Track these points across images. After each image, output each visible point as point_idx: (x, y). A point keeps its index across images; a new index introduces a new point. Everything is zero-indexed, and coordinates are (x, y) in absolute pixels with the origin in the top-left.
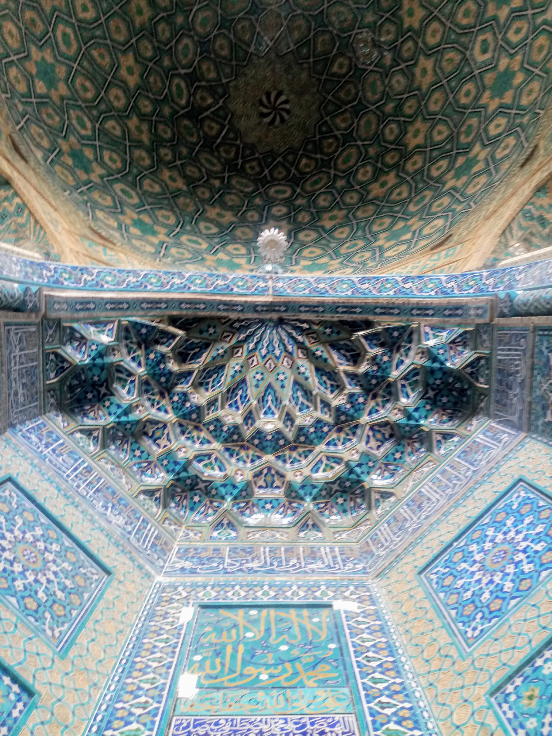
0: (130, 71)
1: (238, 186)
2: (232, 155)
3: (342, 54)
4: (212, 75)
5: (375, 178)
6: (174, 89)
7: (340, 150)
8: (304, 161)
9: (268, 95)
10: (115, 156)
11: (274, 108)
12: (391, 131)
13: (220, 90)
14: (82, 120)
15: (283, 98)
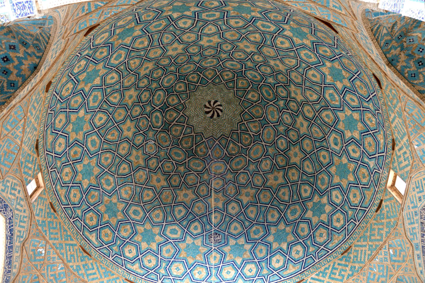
0: (129, 129)
1: (194, 167)
2: (190, 144)
3: (254, 91)
4: (176, 101)
5: (271, 171)
6: (154, 120)
7: (252, 144)
8: (231, 145)
9: (209, 102)
10: (127, 188)
11: (213, 108)
12: (282, 144)
13: (180, 107)
14: (108, 180)
15: (218, 103)
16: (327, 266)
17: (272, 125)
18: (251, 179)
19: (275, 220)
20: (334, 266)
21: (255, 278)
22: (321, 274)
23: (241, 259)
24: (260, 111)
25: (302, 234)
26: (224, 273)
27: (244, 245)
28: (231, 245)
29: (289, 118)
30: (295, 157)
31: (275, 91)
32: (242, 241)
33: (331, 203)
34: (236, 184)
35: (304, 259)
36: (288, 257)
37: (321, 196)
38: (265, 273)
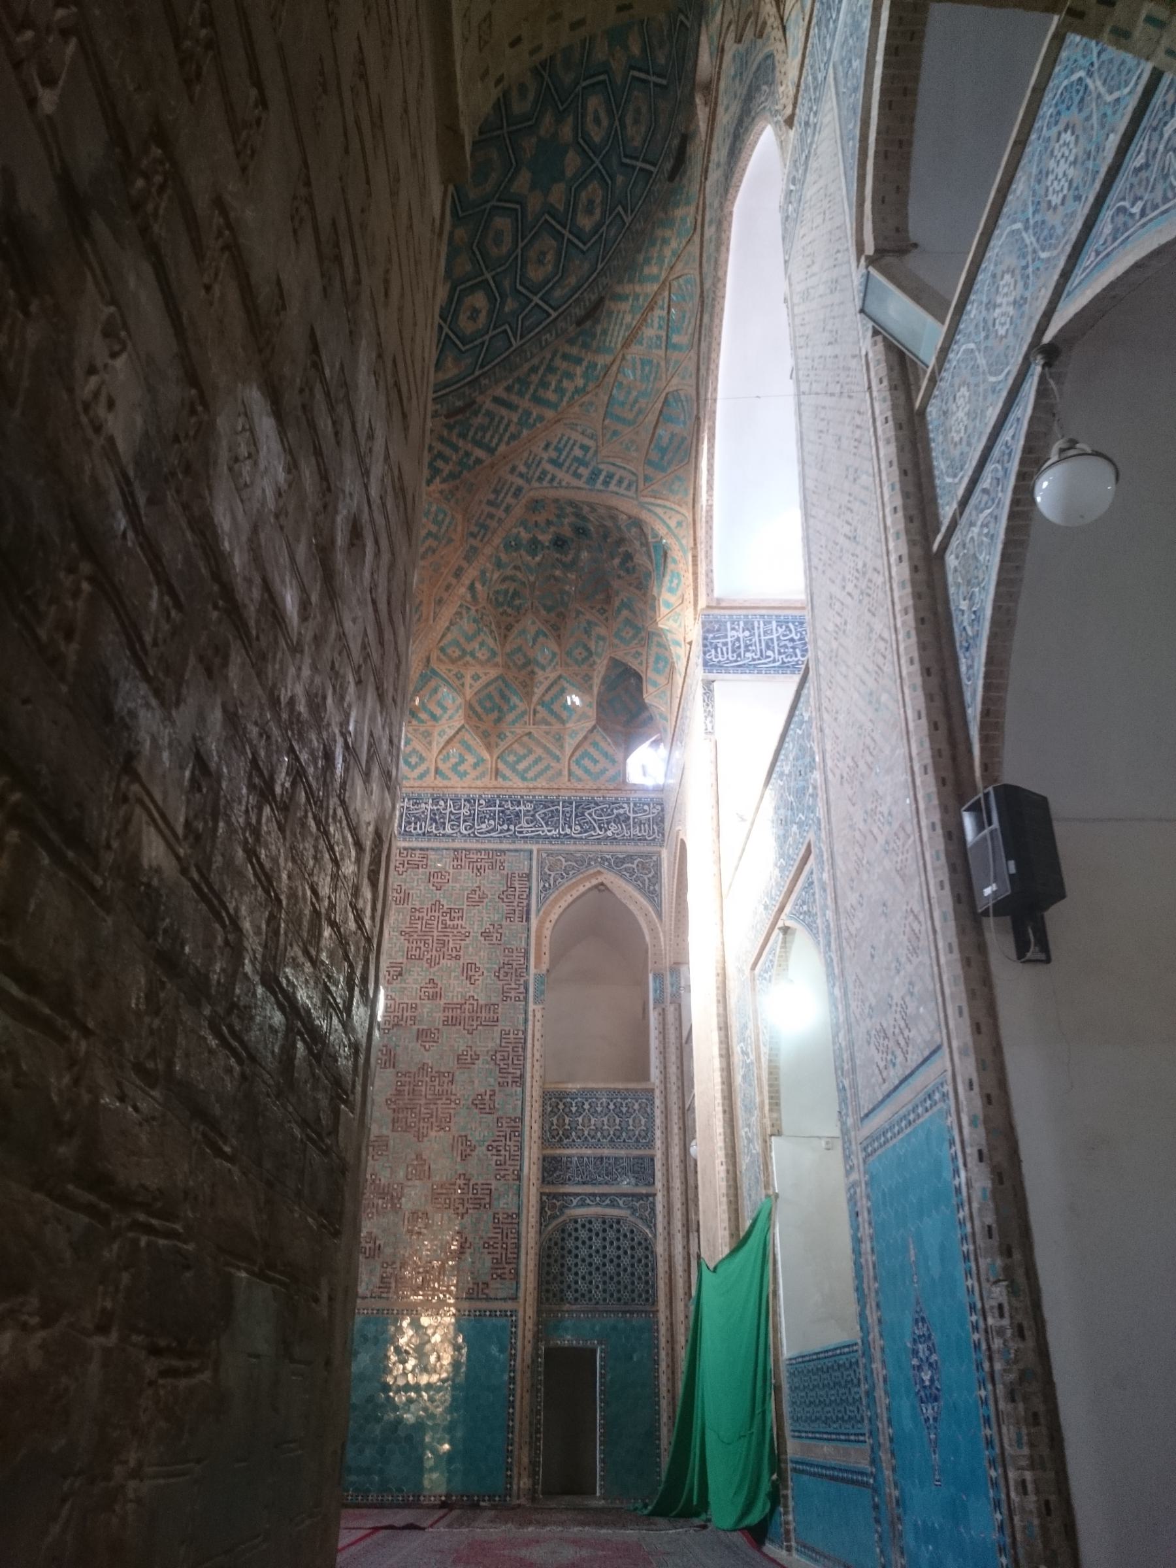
16: (535, 361)
20: (552, 360)
22: (517, 386)
25: (494, 252)
35: (487, 338)
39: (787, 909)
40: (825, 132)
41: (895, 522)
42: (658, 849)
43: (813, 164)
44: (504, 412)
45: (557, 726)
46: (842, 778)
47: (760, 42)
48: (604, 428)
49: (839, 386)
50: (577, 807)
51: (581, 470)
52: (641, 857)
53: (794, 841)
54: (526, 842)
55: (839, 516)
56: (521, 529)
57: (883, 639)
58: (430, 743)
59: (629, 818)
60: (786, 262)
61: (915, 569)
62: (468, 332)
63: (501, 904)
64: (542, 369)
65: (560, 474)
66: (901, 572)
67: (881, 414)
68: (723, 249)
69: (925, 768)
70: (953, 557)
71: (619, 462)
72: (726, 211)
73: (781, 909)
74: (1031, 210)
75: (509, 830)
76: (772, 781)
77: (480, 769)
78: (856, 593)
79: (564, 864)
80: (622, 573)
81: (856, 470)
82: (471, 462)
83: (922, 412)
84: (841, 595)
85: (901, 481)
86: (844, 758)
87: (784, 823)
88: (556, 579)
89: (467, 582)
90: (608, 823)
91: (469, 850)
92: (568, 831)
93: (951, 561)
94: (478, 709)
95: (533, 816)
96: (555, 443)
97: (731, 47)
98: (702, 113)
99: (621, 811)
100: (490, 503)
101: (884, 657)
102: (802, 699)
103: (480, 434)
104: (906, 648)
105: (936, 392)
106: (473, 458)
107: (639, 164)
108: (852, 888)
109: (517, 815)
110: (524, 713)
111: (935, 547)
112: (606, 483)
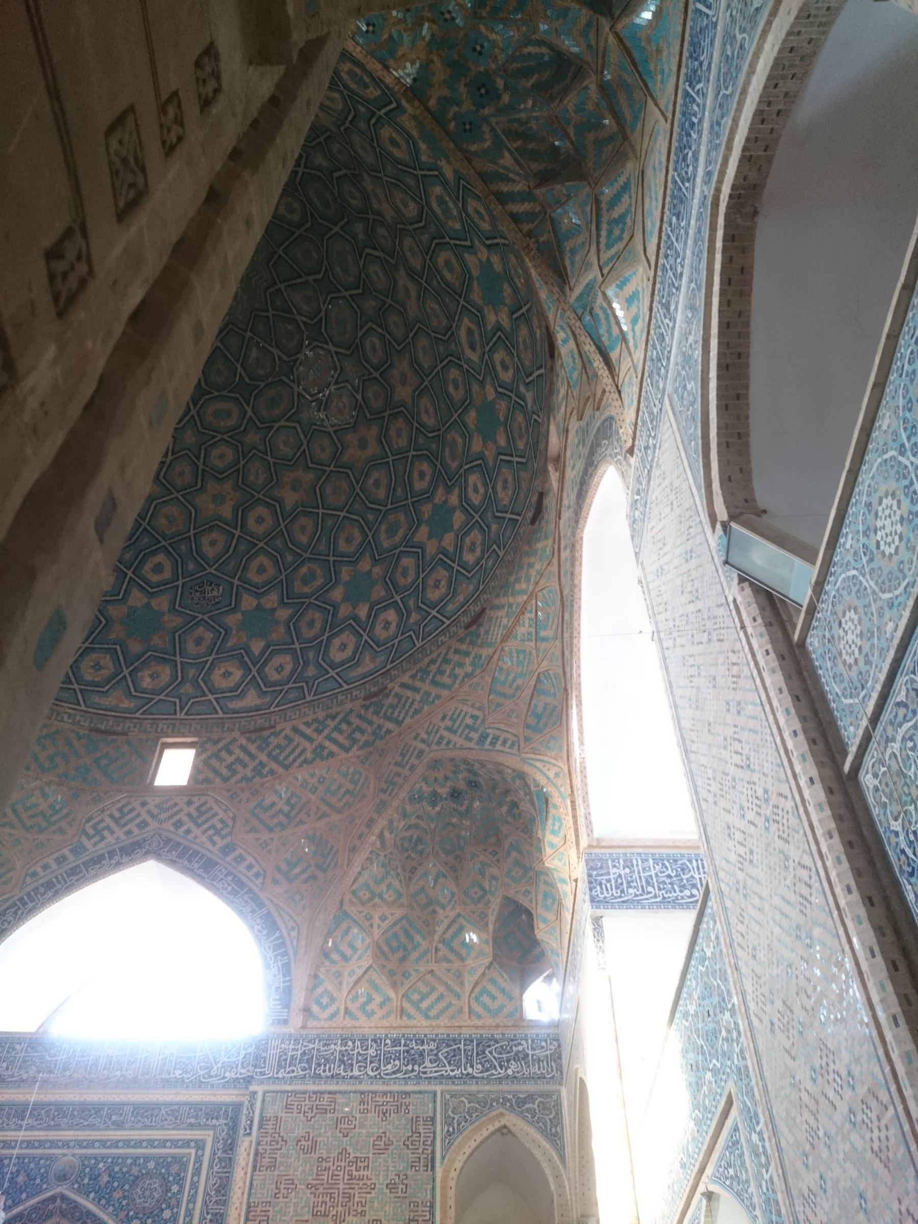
8: (254, 353)
17: (347, 294)
18: (305, 446)
19: (352, 549)
20: (446, 654)
21: (286, 687)
22: (419, 675)
23: (262, 644)
24: (314, 254)
25: (402, 582)
26: (216, 677)
27: (274, 610)
28: (243, 609)
29: (381, 274)
30: (404, 383)
31: (336, 194)
32: (272, 600)
33: (465, 504)
34: (269, 458)
35: (396, 641)
36: (365, 637)
37: (449, 489)
38: (310, 674)
39: (709, 1170)
40: (665, 446)
41: (797, 745)
42: (558, 1087)
43: (656, 473)
44: (409, 693)
45: (457, 964)
46: (772, 1024)
47: (597, 413)
48: (489, 701)
49: (706, 634)
50: (478, 1045)
51: (472, 734)
52: (541, 1096)
53: (710, 1090)
54: (429, 1083)
55: (725, 748)
56: (423, 784)
57: (804, 867)
58: (341, 983)
59: (527, 1055)
60: (636, 553)
61: (830, 791)
62: (382, 638)
63: (406, 1151)
64: (440, 660)
65: (455, 738)
66: (815, 795)
67: (760, 647)
68: (577, 563)
69: (895, 1018)
70: (869, 776)
71: (502, 727)
72: (577, 537)
73: (702, 1170)
74: (904, 436)
75: (413, 1070)
76: (676, 1020)
77: (386, 1009)
78: (760, 822)
79: (468, 1105)
80: (510, 819)
81: (739, 704)
82: (382, 733)
83: (802, 644)
84: (742, 825)
85: (794, 706)
86: (772, 1002)
87: (694, 1068)
88: (454, 826)
89: (377, 831)
90: (508, 1061)
91: (375, 1093)
92: (470, 1070)
93: (868, 780)
94: (385, 949)
95: (436, 1055)
96: (450, 714)
97: (574, 425)
98: (554, 476)
99: (520, 1048)
100: (397, 764)
101: (810, 887)
102: (701, 934)
103: (390, 711)
104: (838, 875)
105: (815, 624)
106: (384, 730)
107: (508, 516)
108: (807, 1166)
109: (421, 1054)
110: (426, 952)
111: (847, 767)
112: (493, 744)
